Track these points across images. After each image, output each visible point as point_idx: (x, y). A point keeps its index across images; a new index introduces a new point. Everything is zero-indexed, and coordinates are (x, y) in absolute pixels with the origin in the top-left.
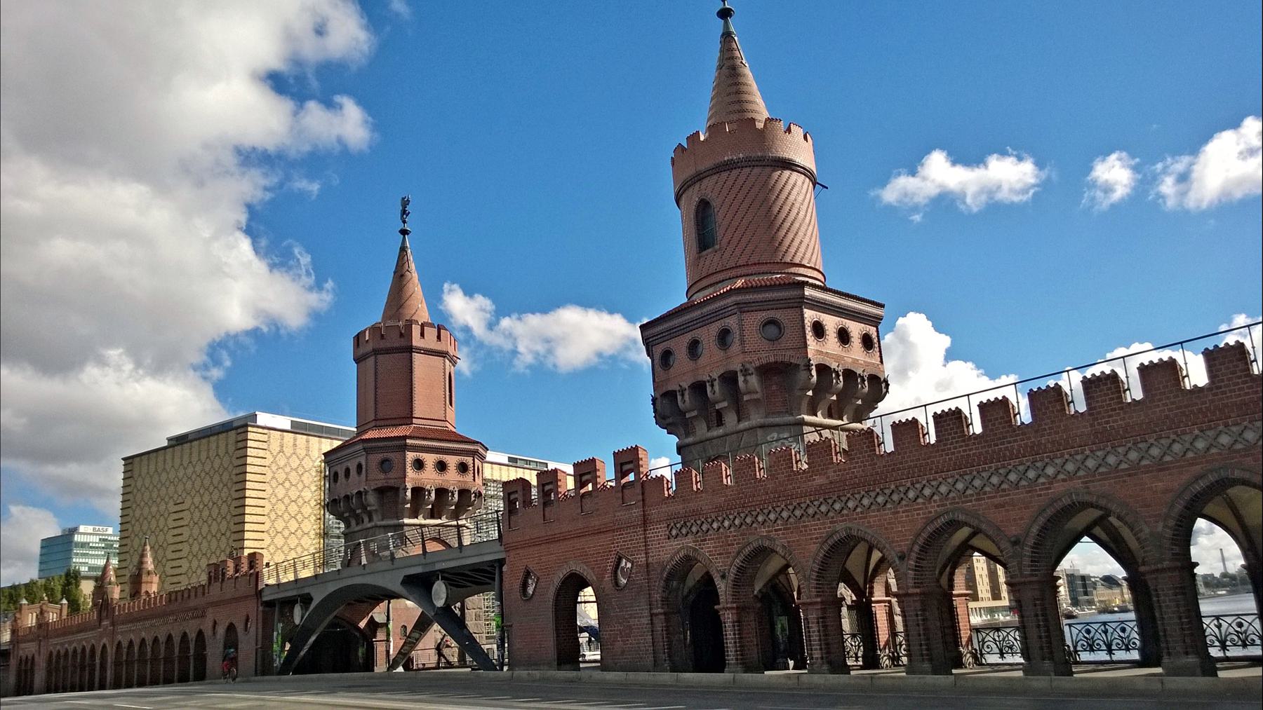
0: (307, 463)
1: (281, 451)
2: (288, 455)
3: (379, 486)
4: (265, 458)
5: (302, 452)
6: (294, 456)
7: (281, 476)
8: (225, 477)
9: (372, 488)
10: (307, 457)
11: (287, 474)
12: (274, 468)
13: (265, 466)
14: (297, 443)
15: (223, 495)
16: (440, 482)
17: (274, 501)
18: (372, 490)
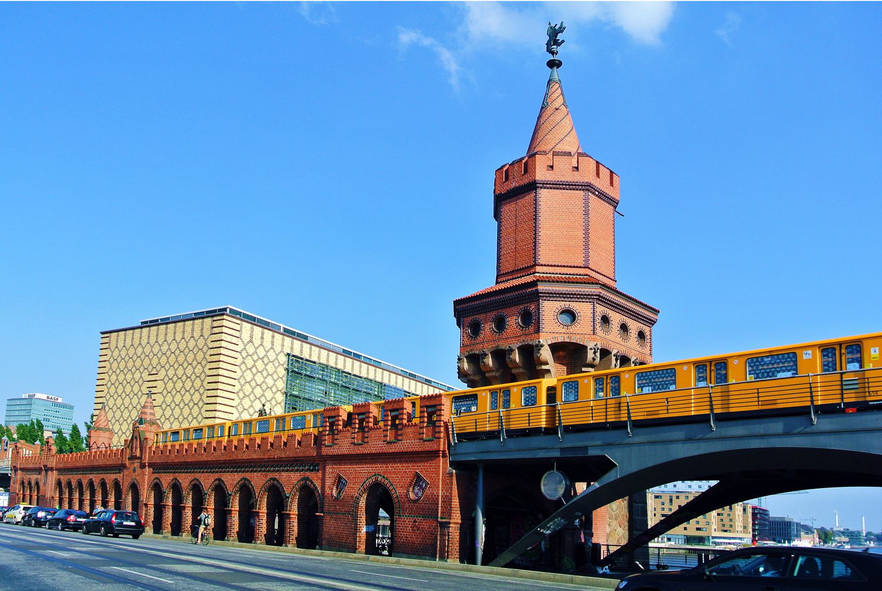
0: (272, 355)
1: (251, 341)
2: (256, 345)
3: (560, 341)
4: (238, 345)
5: (267, 345)
6: (261, 347)
7: (249, 362)
8: (200, 356)
9: (550, 343)
10: (272, 350)
11: (255, 361)
12: (244, 355)
13: (237, 352)
14: (265, 336)
15: (196, 371)
16: (625, 349)
17: (242, 382)
18: (548, 345)
